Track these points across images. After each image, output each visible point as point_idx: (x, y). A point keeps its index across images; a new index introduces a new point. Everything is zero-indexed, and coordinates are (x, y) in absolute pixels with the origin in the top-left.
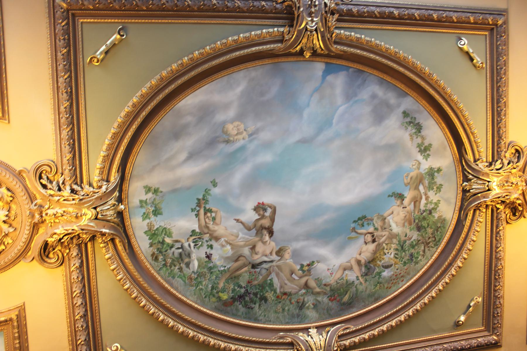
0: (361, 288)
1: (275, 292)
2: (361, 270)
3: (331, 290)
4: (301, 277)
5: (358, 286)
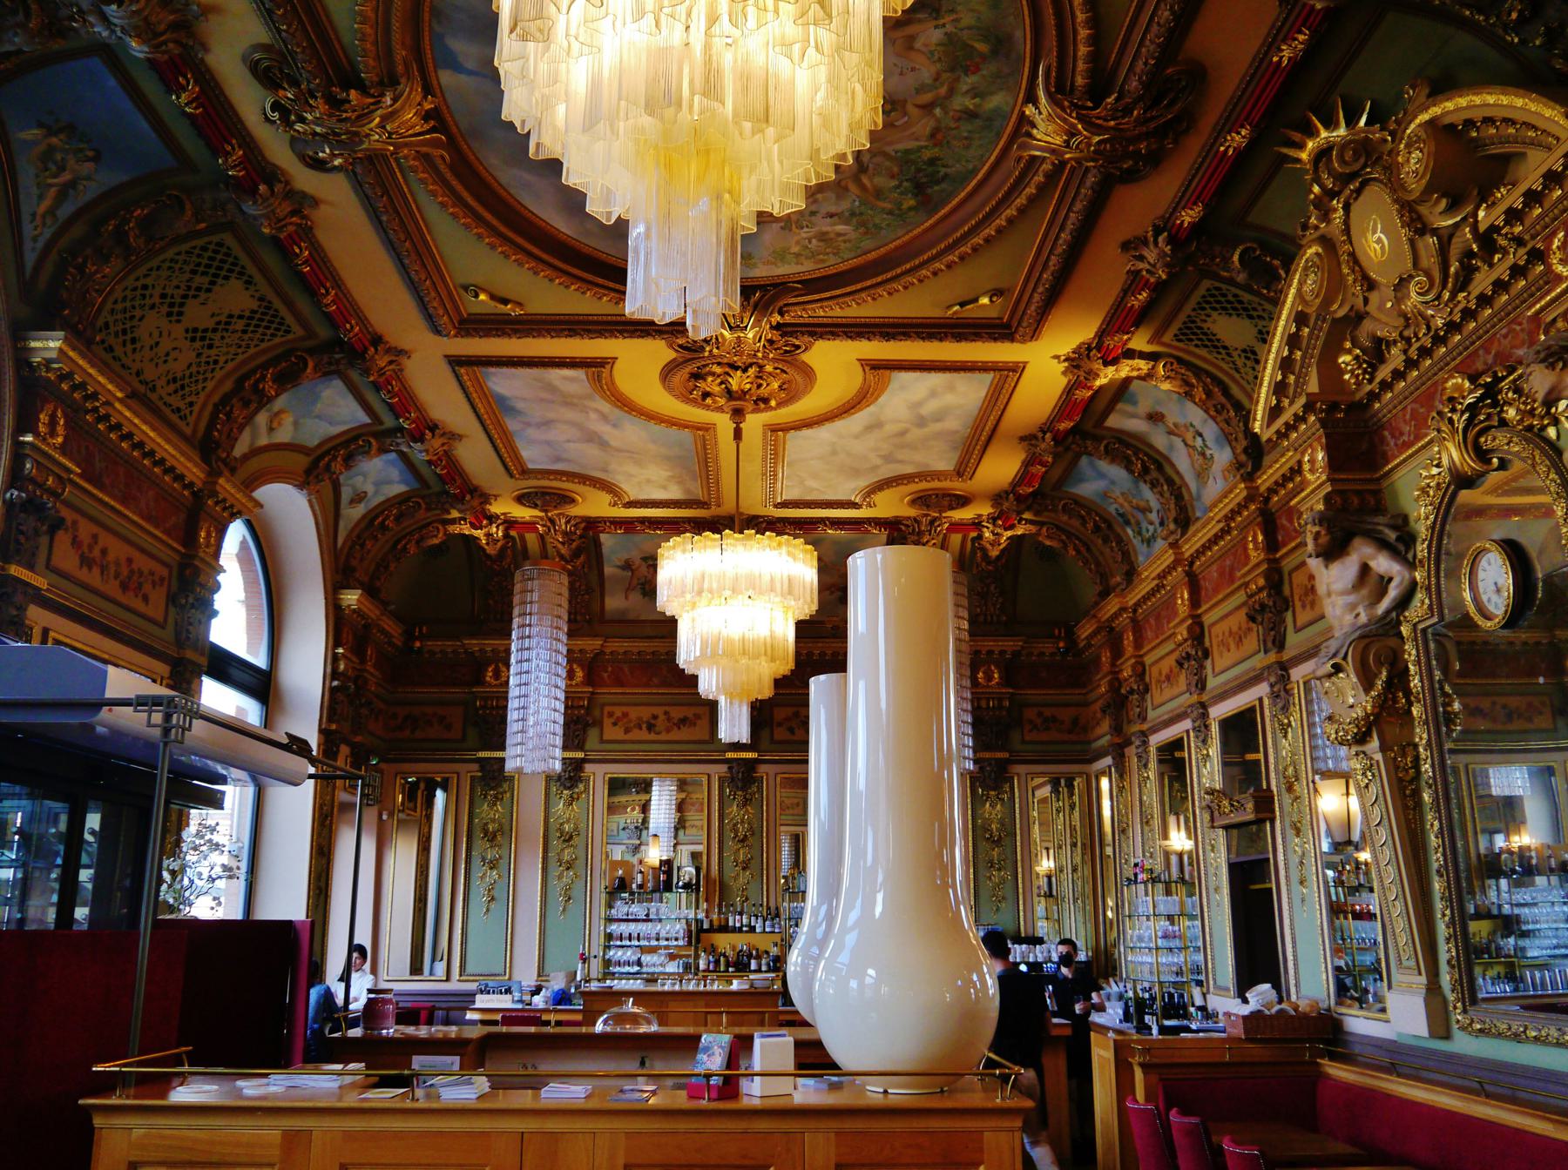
0: (967, 20)
1: (926, 147)
2: (920, 21)
3: (952, 69)
4: (905, 114)
5: (960, 26)
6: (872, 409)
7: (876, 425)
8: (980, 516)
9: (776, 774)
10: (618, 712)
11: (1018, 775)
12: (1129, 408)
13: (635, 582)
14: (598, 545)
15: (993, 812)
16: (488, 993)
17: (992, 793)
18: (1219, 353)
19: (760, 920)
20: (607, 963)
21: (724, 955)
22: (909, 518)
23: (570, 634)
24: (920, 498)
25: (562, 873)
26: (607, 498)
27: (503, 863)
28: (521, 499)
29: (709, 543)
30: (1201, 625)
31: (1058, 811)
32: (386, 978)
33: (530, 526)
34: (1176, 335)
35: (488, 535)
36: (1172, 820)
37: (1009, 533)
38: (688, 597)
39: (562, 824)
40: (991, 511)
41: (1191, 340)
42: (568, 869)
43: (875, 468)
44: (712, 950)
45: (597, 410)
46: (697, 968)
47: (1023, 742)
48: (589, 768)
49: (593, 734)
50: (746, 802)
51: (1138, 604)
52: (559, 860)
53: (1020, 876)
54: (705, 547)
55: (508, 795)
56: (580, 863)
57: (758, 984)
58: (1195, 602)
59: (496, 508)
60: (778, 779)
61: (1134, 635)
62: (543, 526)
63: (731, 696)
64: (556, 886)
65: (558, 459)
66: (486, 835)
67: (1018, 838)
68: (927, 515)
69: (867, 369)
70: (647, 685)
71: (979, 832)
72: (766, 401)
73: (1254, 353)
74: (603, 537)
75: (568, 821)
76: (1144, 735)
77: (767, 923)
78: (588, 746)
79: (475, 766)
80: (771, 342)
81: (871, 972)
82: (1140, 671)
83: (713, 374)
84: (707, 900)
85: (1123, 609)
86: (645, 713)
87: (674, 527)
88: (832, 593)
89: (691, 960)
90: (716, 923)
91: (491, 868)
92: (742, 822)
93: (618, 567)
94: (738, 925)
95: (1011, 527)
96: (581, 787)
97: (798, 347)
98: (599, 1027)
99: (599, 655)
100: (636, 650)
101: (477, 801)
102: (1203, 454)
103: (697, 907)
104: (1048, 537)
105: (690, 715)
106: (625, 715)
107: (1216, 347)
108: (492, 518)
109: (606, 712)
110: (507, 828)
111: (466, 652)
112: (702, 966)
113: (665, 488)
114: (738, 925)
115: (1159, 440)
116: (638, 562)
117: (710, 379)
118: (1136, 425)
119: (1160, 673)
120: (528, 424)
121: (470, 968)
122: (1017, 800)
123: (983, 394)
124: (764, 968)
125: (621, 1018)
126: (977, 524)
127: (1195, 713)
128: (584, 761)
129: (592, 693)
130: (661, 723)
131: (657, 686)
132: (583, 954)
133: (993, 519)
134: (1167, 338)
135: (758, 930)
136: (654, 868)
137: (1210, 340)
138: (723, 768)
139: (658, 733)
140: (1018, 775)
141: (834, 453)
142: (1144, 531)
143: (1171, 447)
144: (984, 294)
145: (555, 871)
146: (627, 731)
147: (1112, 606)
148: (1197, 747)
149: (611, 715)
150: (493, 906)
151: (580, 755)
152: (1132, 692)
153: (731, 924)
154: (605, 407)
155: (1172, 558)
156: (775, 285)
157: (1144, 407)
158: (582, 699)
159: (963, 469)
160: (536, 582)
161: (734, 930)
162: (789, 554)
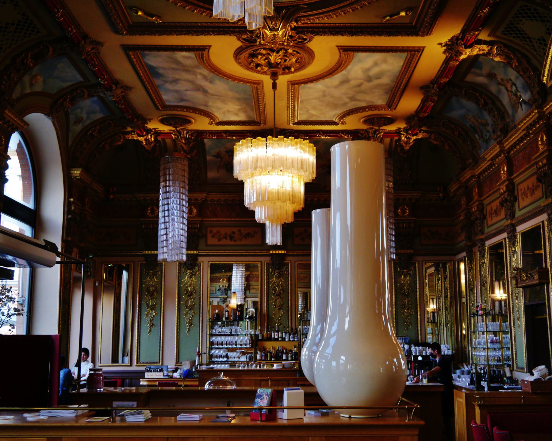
6: (344, 72)
7: (346, 81)
8: (400, 129)
9: (295, 262)
10: (215, 230)
12: (478, 71)
14: (203, 144)
15: (405, 279)
16: (151, 371)
17: (405, 270)
18: (526, 41)
20: (211, 356)
21: (270, 352)
22: (363, 130)
23: (190, 191)
25: (187, 312)
26: (207, 120)
28: (163, 121)
29: (260, 143)
30: (513, 184)
31: (438, 280)
32: (99, 365)
33: (168, 134)
34: (503, 32)
35: (146, 140)
36: (496, 284)
37: (415, 138)
38: (250, 170)
40: (405, 126)
41: (511, 34)
42: (190, 310)
43: (345, 104)
44: (263, 349)
45: (201, 74)
48: (200, 259)
51: (481, 174)
52: (186, 306)
54: (258, 145)
55: (159, 273)
57: (286, 366)
58: (510, 172)
59: (151, 126)
60: (296, 264)
61: (478, 190)
63: (272, 222)
65: (182, 100)
67: (418, 293)
68: (372, 128)
69: (341, 51)
72: (289, 68)
73: (544, 41)
74: (206, 141)
75: (190, 286)
76: (483, 241)
77: (291, 336)
79: (143, 259)
80: (291, 37)
81: (343, 357)
82: (481, 208)
83: (261, 54)
84: (261, 325)
85: (473, 176)
86: (229, 231)
87: (242, 135)
89: (253, 355)
90: (265, 336)
92: (278, 284)
93: (214, 156)
94: (276, 337)
95: (416, 134)
96: (197, 268)
97: (305, 39)
98: (206, 387)
102: (516, 95)
106: (218, 232)
107: (524, 38)
108: (149, 131)
109: (208, 231)
112: (258, 357)
113: (237, 115)
114: (276, 337)
115: (493, 88)
117: (260, 57)
118: (481, 80)
119: (492, 209)
120: (166, 82)
121: (142, 360)
123: (402, 64)
124: (289, 359)
125: (218, 383)
126: (398, 133)
127: (509, 229)
128: (198, 255)
129: (201, 221)
132: (198, 352)
133: (406, 130)
134: (499, 33)
135: (287, 340)
136: (234, 309)
137: (521, 34)
138: (268, 259)
141: (324, 96)
142: (484, 136)
143: (499, 91)
144: (402, 10)
146: (219, 240)
147: (467, 175)
148: (510, 247)
149: (211, 232)
150: (152, 329)
151: (196, 252)
152: (477, 219)
153: (273, 336)
154: (206, 72)
155: (498, 150)
156: (293, 6)
157: (486, 70)
158: (197, 224)
159: (392, 103)
160: (172, 164)
161: (274, 340)
162: (301, 148)
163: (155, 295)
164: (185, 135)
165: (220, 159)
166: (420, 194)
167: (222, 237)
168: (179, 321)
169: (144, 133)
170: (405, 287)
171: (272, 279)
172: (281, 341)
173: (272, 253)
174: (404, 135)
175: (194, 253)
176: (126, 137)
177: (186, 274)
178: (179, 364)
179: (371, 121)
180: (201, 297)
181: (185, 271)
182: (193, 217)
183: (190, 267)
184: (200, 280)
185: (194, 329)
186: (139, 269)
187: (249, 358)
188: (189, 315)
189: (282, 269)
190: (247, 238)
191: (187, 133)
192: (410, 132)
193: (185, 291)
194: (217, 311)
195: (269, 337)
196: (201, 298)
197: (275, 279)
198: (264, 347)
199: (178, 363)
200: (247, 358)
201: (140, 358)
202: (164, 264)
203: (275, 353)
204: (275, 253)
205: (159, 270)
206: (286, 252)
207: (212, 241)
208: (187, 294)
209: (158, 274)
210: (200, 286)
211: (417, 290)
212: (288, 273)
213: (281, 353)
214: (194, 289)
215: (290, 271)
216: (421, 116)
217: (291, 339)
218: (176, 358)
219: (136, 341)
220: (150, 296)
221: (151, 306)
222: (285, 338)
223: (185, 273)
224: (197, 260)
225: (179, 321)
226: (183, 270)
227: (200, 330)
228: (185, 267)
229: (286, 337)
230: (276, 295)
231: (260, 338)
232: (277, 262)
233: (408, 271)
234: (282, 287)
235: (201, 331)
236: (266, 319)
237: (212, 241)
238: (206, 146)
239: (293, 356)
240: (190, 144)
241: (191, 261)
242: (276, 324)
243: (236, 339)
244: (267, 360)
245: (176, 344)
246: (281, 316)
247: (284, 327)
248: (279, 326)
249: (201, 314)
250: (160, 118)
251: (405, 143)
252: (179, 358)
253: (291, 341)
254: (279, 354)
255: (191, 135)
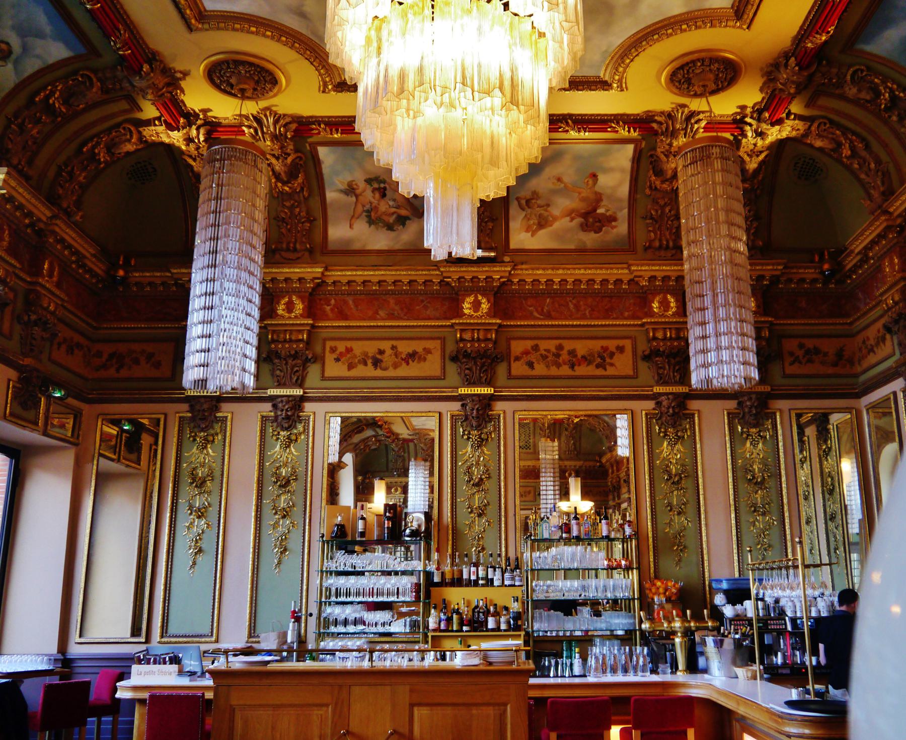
8: (743, 107)
10: (341, 347)
11: (781, 411)
13: (360, 209)
14: (317, 162)
16: (149, 663)
19: (498, 572)
20: (326, 622)
21: (457, 612)
22: (662, 113)
24: (682, 67)
25: (277, 523)
27: (213, 511)
31: (802, 462)
35: (189, 140)
39: (278, 468)
42: (284, 517)
46: (426, 627)
47: (785, 376)
48: (309, 407)
49: (313, 371)
50: (481, 443)
53: (787, 521)
55: (220, 437)
56: (299, 510)
62: (249, 127)
64: (270, 537)
66: (194, 480)
67: (784, 479)
68: (684, 106)
70: (373, 318)
71: (740, 474)
74: (322, 151)
75: (285, 465)
77: (507, 575)
78: (309, 382)
79: (185, 407)
84: (438, 550)
86: (371, 348)
88: (572, 219)
89: (420, 619)
90: (448, 576)
91: (199, 517)
92: (478, 464)
93: (341, 191)
96: (300, 427)
99: (320, 284)
100: (360, 280)
101: (186, 443)
103: (428, 557)
104: (819, 136)
105: (420, 350)
106: (349, 350)
108: (191, 117)
109: (328, 349)
110: (217, 473)
111: (176, 284)
112: (432, 623)
114: (473, 577)
116: (362, 185)
122: (780, 438)
124: (503, 626)
126: (738, 123)
128: (303, 399)
129: (313, 326)
130: (388, 358)
131: (383, 319)
132: (294, 612)
133: (758, 112)
135: (496, 583)
138: (456, 406)
139: (386, 369)
140: (781, 411)
145: (269, 518)
146: (351, 367)
149: (333, 350)
150: (200, 558)
151: (298, 392)
153: (465, 576)
161: (470, 583)
163: (209, 484)
164: (272, 130)
165: (354, 199)
166: (780, 267)
167: (357, 361)
168: (259, 543)
169: (182, 120)
170: (755, 467)
171: (464, 451)
172: (483, 585)
173: (463, 392)
174: (751, 125)
175: (295, 393)
176: (145, 133)
177: (278, 439)
178: (254, 640)
179: (688, 71)
180: (309, 488)
181: (276, 433)
182: (296, 317)
183: (286, 425)
184: (307, 453)
185: (292, 561)
186: (176, 429)
187: (410, 626)
188: (280, 529)
189: (486, 428)
190: (410, 361)
191: (276, 122)
192: (767, 115)
193: (272, 476)
194: (339, 519)
195: (456, 577)
196: (309, 492)
197: (469, 449)
198: (444, 600)
199: (254, 637)
200: (405, 626)
201: (169, 624)
202: (229, 418)
203: (470, 613)
204: (469, 392)
205: (218, 431)
206: (495, 391)
207: (334, 368)
208: (279, 483)
209: (216, 440)
210: (307, 465)
211: (780, 472)
212: (499, 437)
213: (483, 613)
214: (294, 473)
215: (502, 433)
216: (809, 45)
217: (507, 583)
218: (250, 625)
219: (162, 587)
220: (196, 486)
221: (199, 509)
222: (492, 580)
223: (275, 438)
224: (301, 409)
225: (259, 543)
226: (271, 431)
227: (303, 561)
228: (275, 424)
229: (495, 578)
230: (473, 485)
231: (437, 579)
232: (475, 412)
233: (760, 431)
234: (485, 466)
235: (306, 564)
236: (450, 538)
237: (334, 368)
238: (323, 166)
239: (512, 622)
240: (286, 159)
241: (287, 410)
242: (472, 548)
243: (382, 582)
244: (452, 631)
245: (249, 593)
246: (484, 531)
247: (491, 555)
248: (479, 552)
249: (307, 527)
250: (205, 62)
251: (748, 155)
252: (255, 626)
253: (506, 586)
254: (479, 615)
255: (285, 126)
